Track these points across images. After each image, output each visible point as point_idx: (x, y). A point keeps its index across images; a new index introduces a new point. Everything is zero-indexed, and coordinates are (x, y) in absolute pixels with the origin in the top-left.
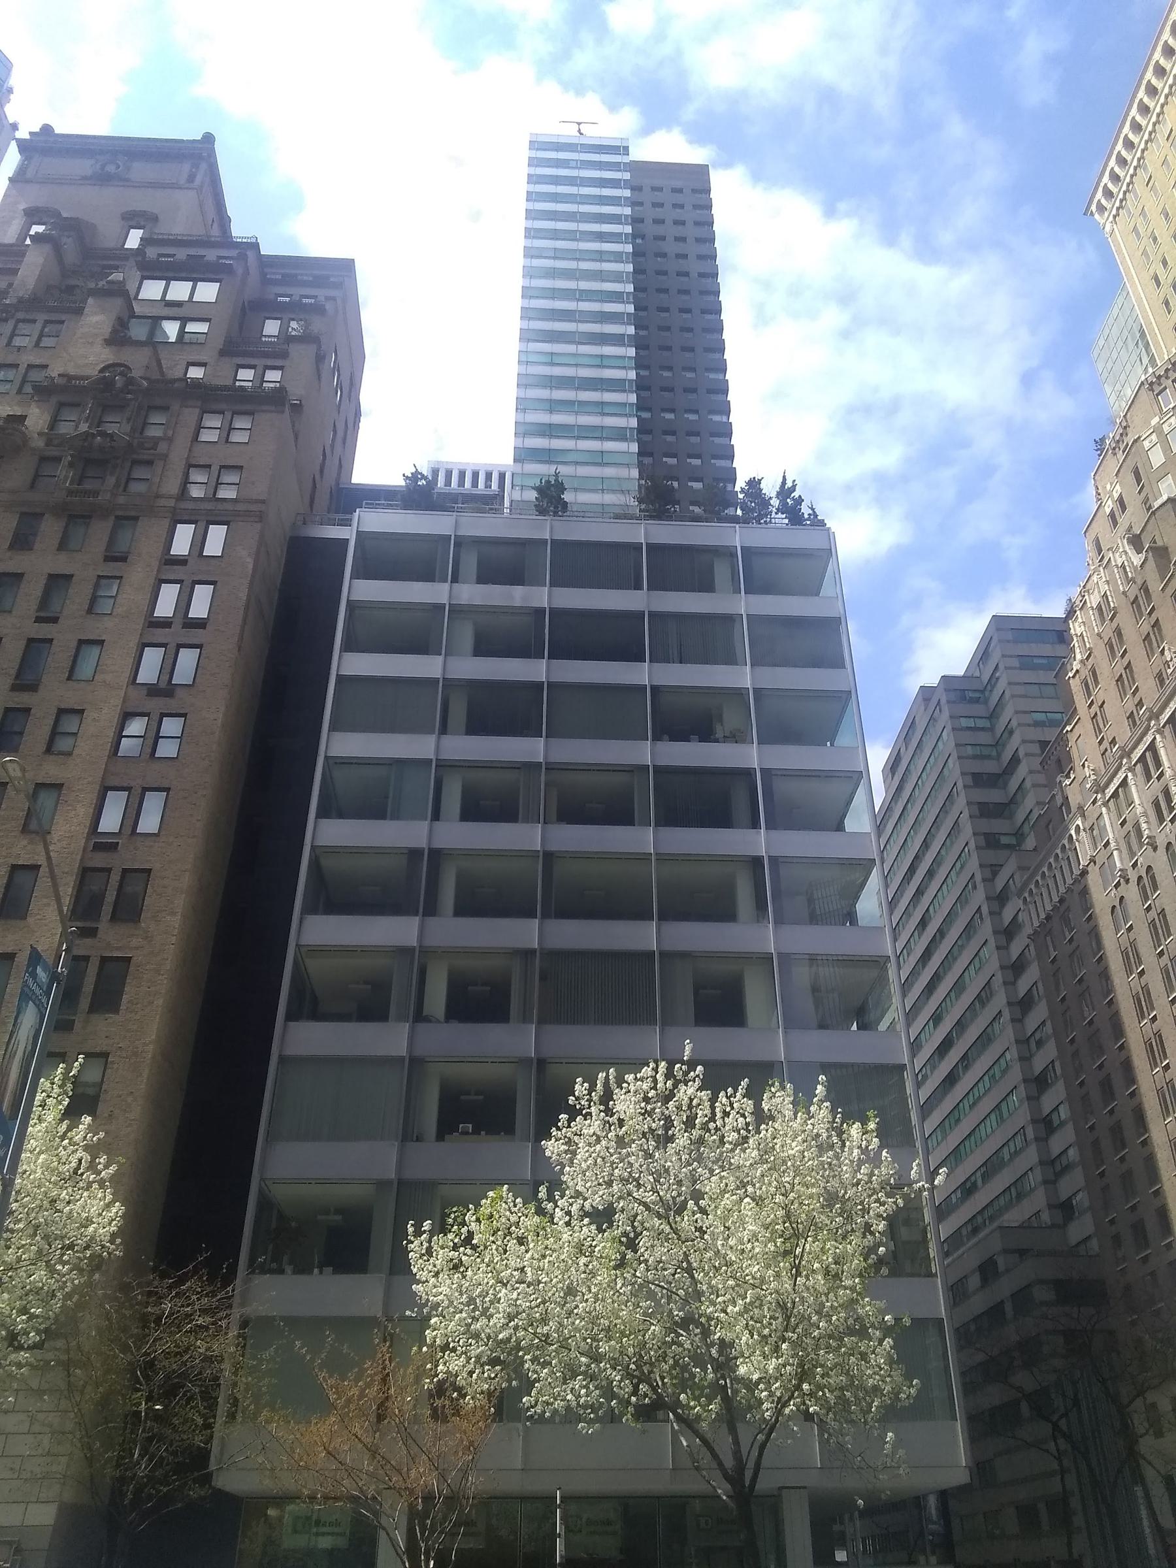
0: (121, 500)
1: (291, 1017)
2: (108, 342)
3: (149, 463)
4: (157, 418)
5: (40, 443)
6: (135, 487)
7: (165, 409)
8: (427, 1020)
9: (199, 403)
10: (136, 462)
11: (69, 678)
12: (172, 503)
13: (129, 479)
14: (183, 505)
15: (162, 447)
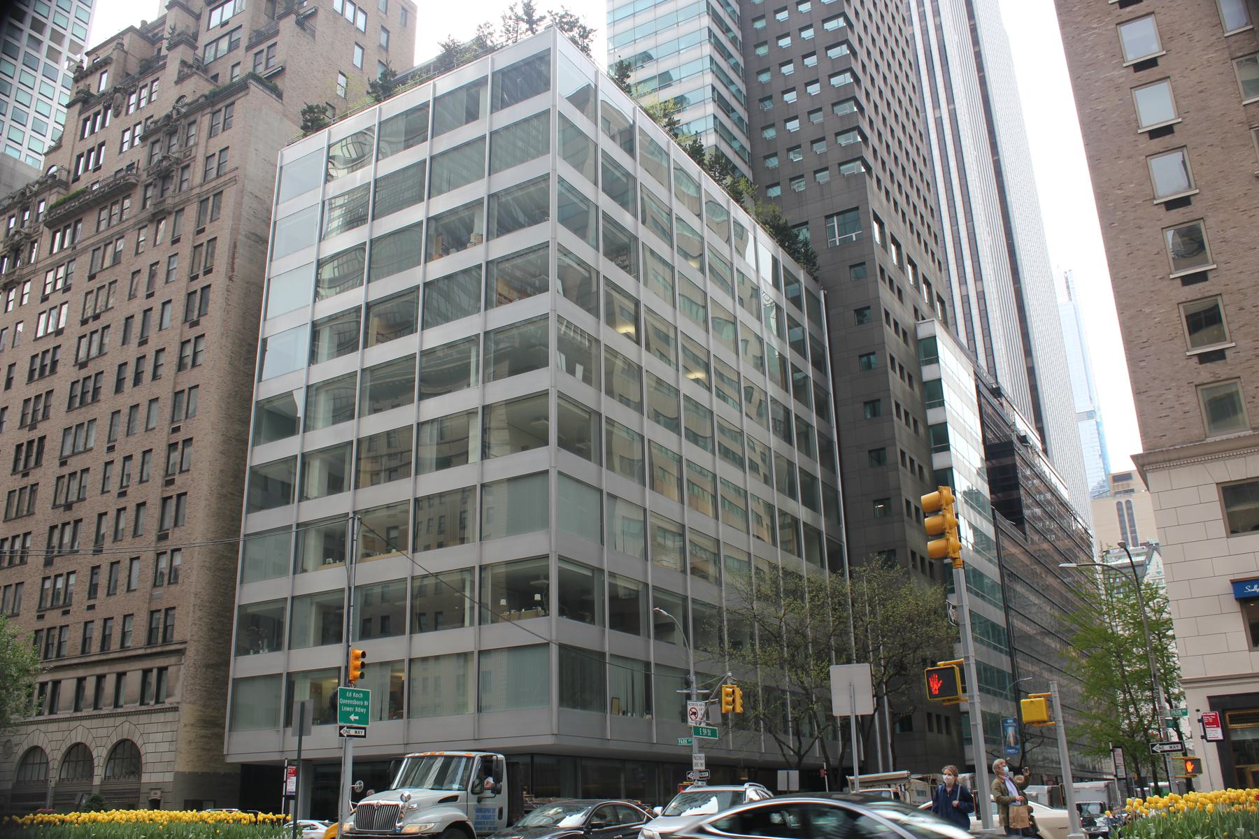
0: (177, 200)
1: (248, 512)
2: (177, 83)
3: (188, 166)
4: (193, 131)
5: (144, 176)
6: (185, 186)
7: (194, 122)
8: (307, 499)
9: (209, 110)
10: (184, 169)
11: (160, 329)
12: (197, 191)
13: (182, 182)
14: (205, 188)
15: (194, 149)
